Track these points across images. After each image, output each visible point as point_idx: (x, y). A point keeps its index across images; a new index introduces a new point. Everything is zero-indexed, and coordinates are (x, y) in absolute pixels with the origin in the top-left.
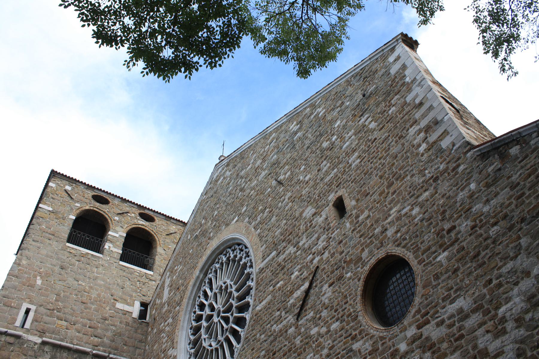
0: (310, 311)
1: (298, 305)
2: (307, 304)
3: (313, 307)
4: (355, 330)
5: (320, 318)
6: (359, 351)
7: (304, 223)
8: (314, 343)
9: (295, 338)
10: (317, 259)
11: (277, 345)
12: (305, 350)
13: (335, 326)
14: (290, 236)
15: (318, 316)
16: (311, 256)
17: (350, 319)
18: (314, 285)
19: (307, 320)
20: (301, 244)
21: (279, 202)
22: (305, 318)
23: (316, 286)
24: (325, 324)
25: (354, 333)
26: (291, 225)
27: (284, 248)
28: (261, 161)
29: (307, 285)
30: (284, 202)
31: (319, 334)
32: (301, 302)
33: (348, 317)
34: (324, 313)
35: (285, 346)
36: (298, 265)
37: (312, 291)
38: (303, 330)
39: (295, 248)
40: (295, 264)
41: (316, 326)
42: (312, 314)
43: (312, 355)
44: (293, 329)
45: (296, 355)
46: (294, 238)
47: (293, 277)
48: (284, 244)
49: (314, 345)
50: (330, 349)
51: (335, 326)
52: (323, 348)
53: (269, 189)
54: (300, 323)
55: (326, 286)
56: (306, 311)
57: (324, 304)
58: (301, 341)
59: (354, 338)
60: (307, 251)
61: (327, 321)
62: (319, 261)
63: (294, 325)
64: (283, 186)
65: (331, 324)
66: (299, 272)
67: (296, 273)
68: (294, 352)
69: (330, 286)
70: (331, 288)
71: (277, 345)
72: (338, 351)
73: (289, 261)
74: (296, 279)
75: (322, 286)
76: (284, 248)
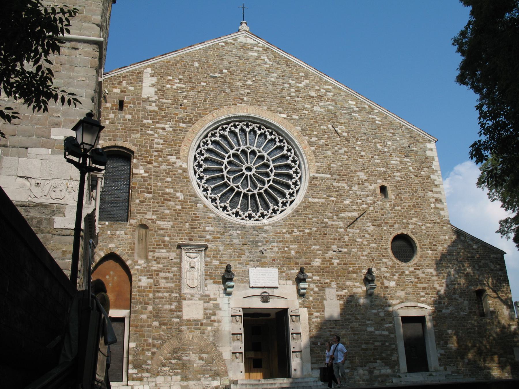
0: (357, 228)
1: (348, 220)
2: (355, 224)
3: (360, 228)
4: (385, 253)
5: (364, 236)
6: (386, 263)
7: (357, 178)
8: (358, 245)
9: (344, 235)
10: (364, 206)
11: (328, 231)
12: (351, 245)
13: (374, 245)
14: (345, 177)
15: (362, 234)
16: (360, 201)
17: (383, 247)
18: (361, 217)
19: (354, 232)
20: (353, 188)
21: (336, 146)
22: (354, 230)
23: (363, 219)
24: (367, 241)
25: (384, 254)
26: (346, 170)
27: (339, 180)
28: (317, 95)
29: (356, 214)
30: (340, 151)
31: (362, 243)
32: (351, 221)
33: (382, 246)
34: (367, 236)
35: (335, 235)
36: (350, 198)
37: (359, 219)
38: (350, 235)
39: (348, 188)
40: (347, 196)
41: (361, 238)
42: (358, 231)
43: (356, 250)
44: (342, 230)
45: (344, 244)
46: (348, 180)
47: (345, 202)
48: (338, 177)
49: (358, 246)
50: (369, 253)
51: (374, 245)
52: (364, 251)
53: (325, 127)
54: (348, 230)
55: (369, 224)
56: (354, 226)
57: (368, 231)
58: (349, 240)
59: (384, 256)
60: (360, 197)
61: (369, 241)
62: (366, 208)
63: (343, 228)
64: (340, 138)
65: (371, 243)
66: (350, 202)
67: (348, 202)
68: (343, 242)
69: (373, 225)
70: (374, 227)
71: (328, 231)
72: (374, 257)
73: (343, 191)
74: (348, 205)
75: (367, 222)
76: (339, 180)
